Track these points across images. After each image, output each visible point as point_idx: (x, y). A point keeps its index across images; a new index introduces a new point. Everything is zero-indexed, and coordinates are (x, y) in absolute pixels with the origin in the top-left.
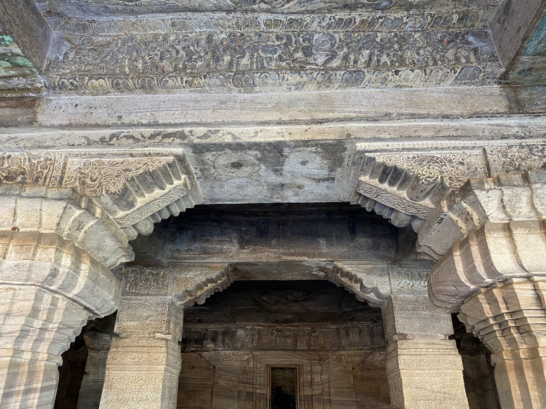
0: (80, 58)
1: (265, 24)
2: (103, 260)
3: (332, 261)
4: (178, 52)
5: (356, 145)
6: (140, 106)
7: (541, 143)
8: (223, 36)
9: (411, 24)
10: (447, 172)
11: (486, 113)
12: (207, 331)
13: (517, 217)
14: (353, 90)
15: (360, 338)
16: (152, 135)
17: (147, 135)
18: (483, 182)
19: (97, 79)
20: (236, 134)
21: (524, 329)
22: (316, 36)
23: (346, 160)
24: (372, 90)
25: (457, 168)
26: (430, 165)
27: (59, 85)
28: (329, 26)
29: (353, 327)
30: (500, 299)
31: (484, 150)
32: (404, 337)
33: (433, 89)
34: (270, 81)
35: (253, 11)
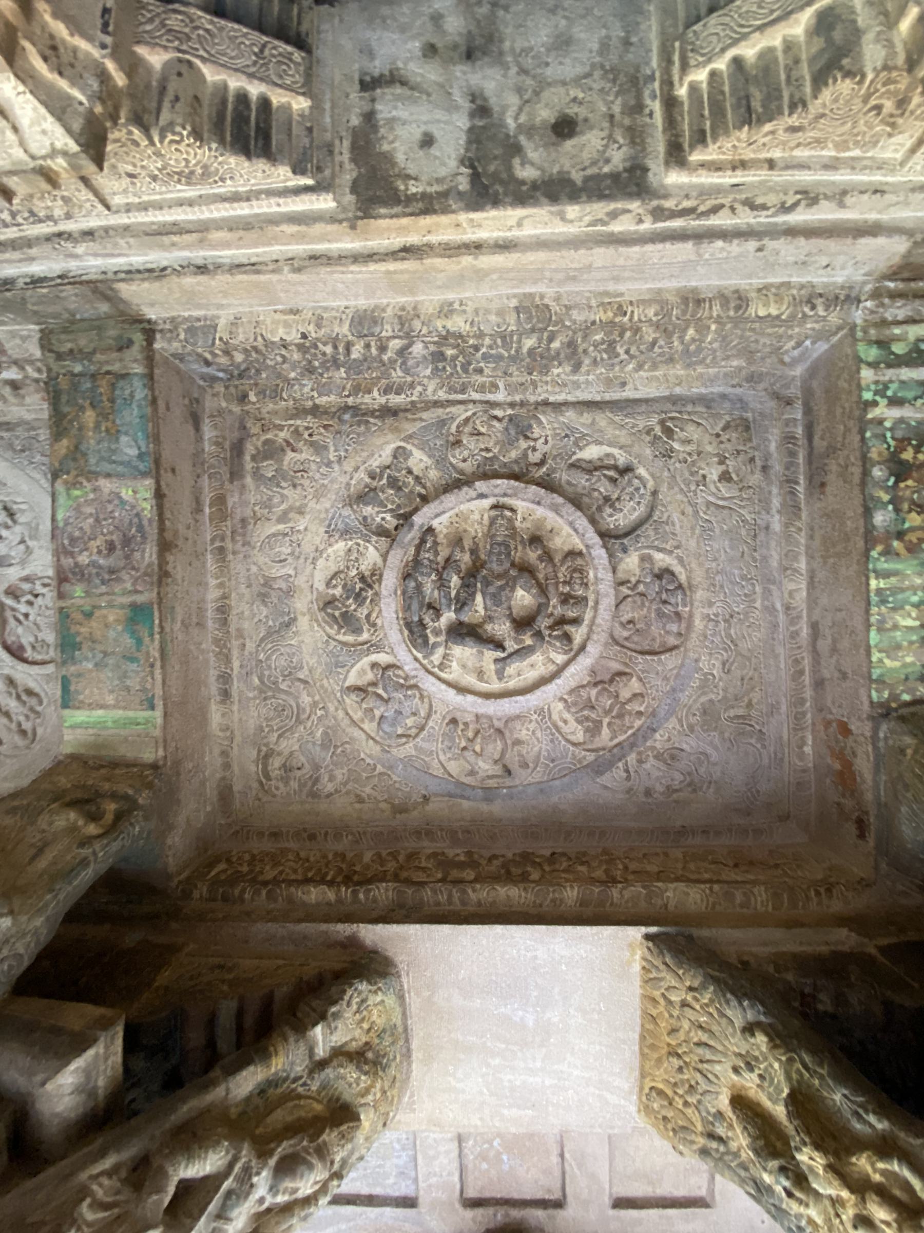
1: (496, 387)
4: (627, 352)
5: (334, 204)
6: (714, 269)
8: (556, 371)
9: (306, 389)
14: (362, 303)
17: (725, 212)
20: (557, 220)
22: (428, 372)
23: (346, 156)
24: (334, 304)
28: (412, 386)
31: (108, 207)
33: (241, 309)
34: (493, 318)
35: (512, 405)
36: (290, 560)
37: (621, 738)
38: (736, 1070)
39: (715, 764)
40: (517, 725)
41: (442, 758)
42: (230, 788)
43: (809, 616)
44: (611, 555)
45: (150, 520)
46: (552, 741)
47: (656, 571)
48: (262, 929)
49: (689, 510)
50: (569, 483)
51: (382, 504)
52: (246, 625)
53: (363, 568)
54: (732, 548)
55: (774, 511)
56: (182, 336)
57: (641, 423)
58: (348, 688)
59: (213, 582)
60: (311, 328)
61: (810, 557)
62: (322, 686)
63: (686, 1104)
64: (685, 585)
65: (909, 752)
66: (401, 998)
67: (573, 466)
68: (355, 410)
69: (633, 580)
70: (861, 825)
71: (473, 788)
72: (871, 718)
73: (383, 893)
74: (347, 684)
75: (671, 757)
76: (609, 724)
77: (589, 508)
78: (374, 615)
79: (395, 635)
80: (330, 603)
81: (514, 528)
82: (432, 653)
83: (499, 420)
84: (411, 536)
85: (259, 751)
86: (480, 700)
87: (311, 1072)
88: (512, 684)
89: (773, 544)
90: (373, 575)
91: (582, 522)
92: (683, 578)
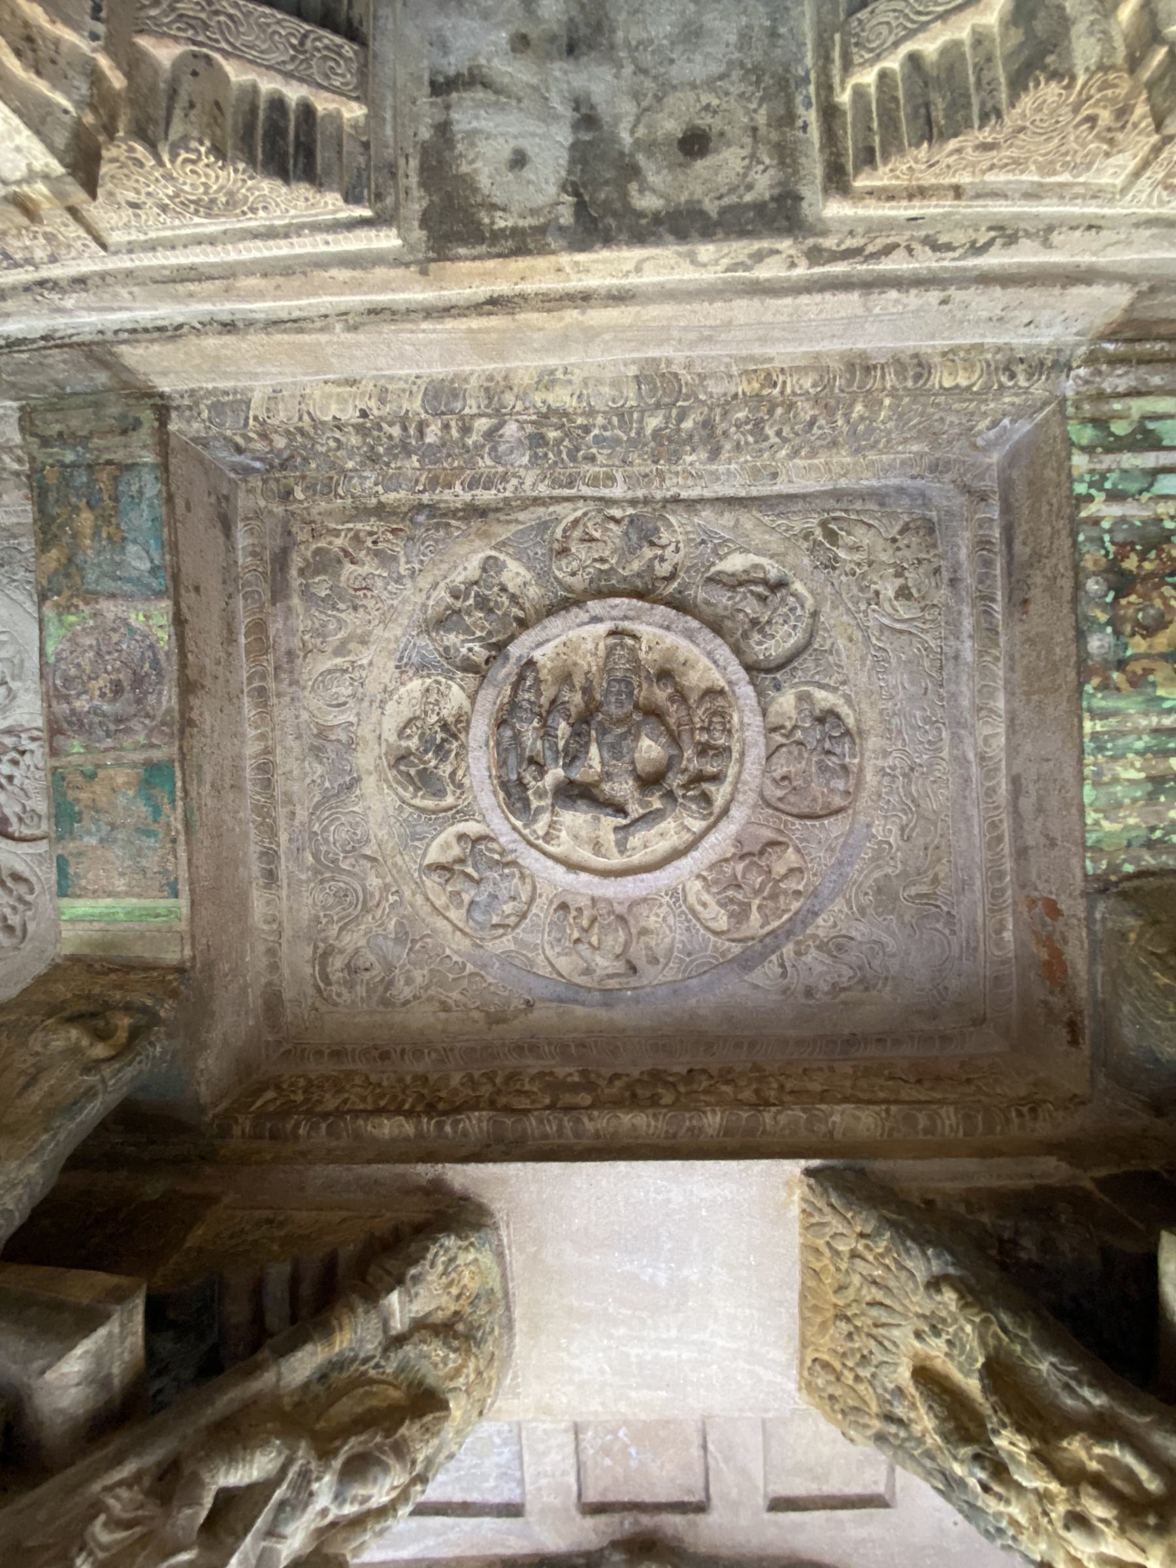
1: (613, 479)
5: (399, 242)
6: (886, 326)
8: (689, 459)
9: (368, 484)
14: (439, 371)
17: (901, 253)
20: (686, 264)
22: (525, 460)
23: (414, 180)
28: (504, 478)
31: (104, 246)
33: (281, 379)
34: (606, 390)
35: (633, 502)
36: (351, 703)
37: (775, 924)
38: (918, 1335)
39: (893, 955)
40: (643, 910)
41: (549, 953)
42: (278, 995)
43: (1009, 767)
44: (760, 693)
45: (167, 654)
46: (688, 929)
47: (817, 713)
48: (320, 1173)
49: (858, 635)
50: (707, 603)
51: (468, 631)
52: (296, 787)
53: (445, 712)
54: (912, 682)
55: (965, 635)
56: (205, 415)
57: (798, 525)
58: (429, 866)
59: (252, 733)
60: (373, 404)
61: (1010, 694)
62: (395, 865)
63: (857, 1378)
64: (854, 730)
65: (1132, 936)
66: (500, 1255)
67: (710, 580)
68: (432, 509)
69: (789, 725)
70: (1074, 1030)
71: (589, 990)
72: (1085, 894)
73: (475, 1123)
74: (427, 862)
75: (836, 947)
76: (760, 907)
77: (732, 634)
78: (460, 773)
79: (487, 798)
80: (403, 757)
81: (637, 660)
82: (535, 821)
83: (617, 521)
84: (505, 672)
85: (316, 948)
86: (596, 880)
87: (386, 1350)
88: (637, 858)
89: (965, 677)
90: (458, 721)
91: (724, 652)
92: (851, 721)
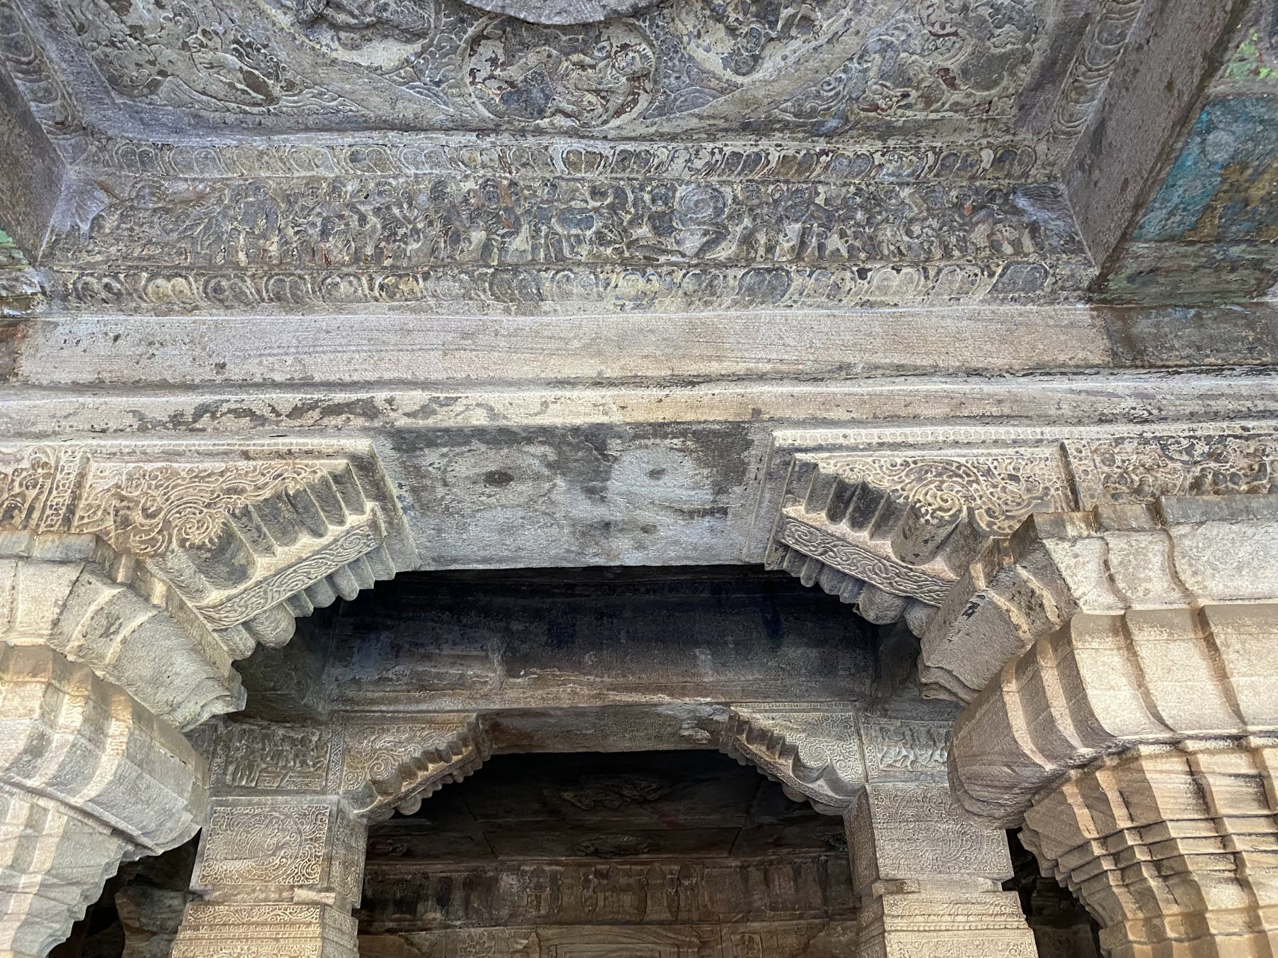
0: (131, 229)
1: (566, 162)
2: (167, 709)
3: (728, 704)
4: (363, 219)
5: (774, 434)
6: (269, 341)
7: (1186, 434)
8: (470, 185)
9: (890, 168)
10: (981, 497)
11: (1064, 365)
12: (427, 878)
13: (1142, 601)
14: (765, 312)
15: (797, 891)
16: (296, 408)
17: (284, 408)
18: (1063, 521)
19: (169, 278)
20: (498, 408)
21: (1172, 868)
23: (753, 467)
24: (807, 311)
25: (1004, 488)
26: (943, 482)
27: (75, 289)
28: (711, 168)
29: (780, 862)
30: (1113, 796)
31: (1062, 447)
32: (898, 886)
33: (946, 310)
35: (539, 132)
45: (1256, 22)
56: (1050, 280)
60: (849, 284)
68: (815, 131)
